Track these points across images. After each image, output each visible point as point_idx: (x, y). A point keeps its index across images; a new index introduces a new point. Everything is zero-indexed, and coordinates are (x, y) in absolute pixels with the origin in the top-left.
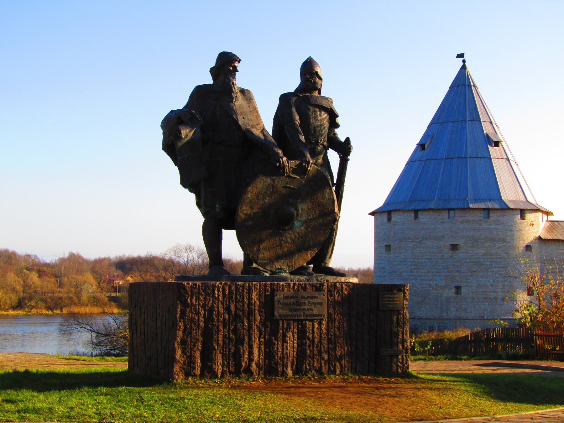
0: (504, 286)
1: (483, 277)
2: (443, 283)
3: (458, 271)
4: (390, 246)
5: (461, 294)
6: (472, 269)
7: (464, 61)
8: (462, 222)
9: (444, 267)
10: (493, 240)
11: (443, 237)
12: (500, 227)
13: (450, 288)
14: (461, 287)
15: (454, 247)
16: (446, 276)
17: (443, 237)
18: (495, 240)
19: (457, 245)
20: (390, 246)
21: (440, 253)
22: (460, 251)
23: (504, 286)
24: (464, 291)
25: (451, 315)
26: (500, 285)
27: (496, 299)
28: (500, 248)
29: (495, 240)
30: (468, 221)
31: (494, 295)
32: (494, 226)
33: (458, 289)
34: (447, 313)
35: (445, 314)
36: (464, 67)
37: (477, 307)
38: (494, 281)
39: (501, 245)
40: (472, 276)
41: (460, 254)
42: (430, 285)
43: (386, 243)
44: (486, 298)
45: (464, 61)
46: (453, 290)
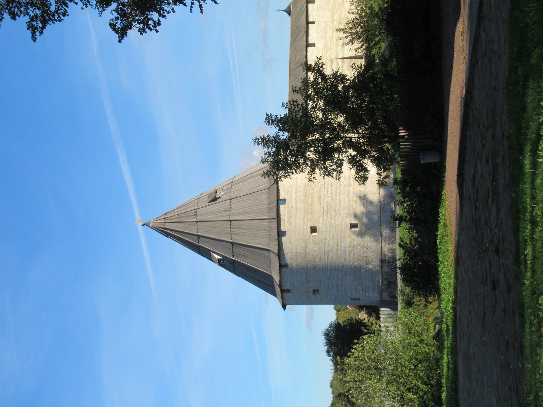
0: (348, 185)
1: (340, 203)
4: (314, 291)
6: (334, 214)
8: (290, 224)
10: (306, 195)
15: (314, 230)
18: (306, 194)
19: (311, 227)
20: (314, 291)
23: (348, 185)
28: (313, 189)
29: (306, 194)
38: (344, 194)
40: (340, 214)
43: (312, 294)
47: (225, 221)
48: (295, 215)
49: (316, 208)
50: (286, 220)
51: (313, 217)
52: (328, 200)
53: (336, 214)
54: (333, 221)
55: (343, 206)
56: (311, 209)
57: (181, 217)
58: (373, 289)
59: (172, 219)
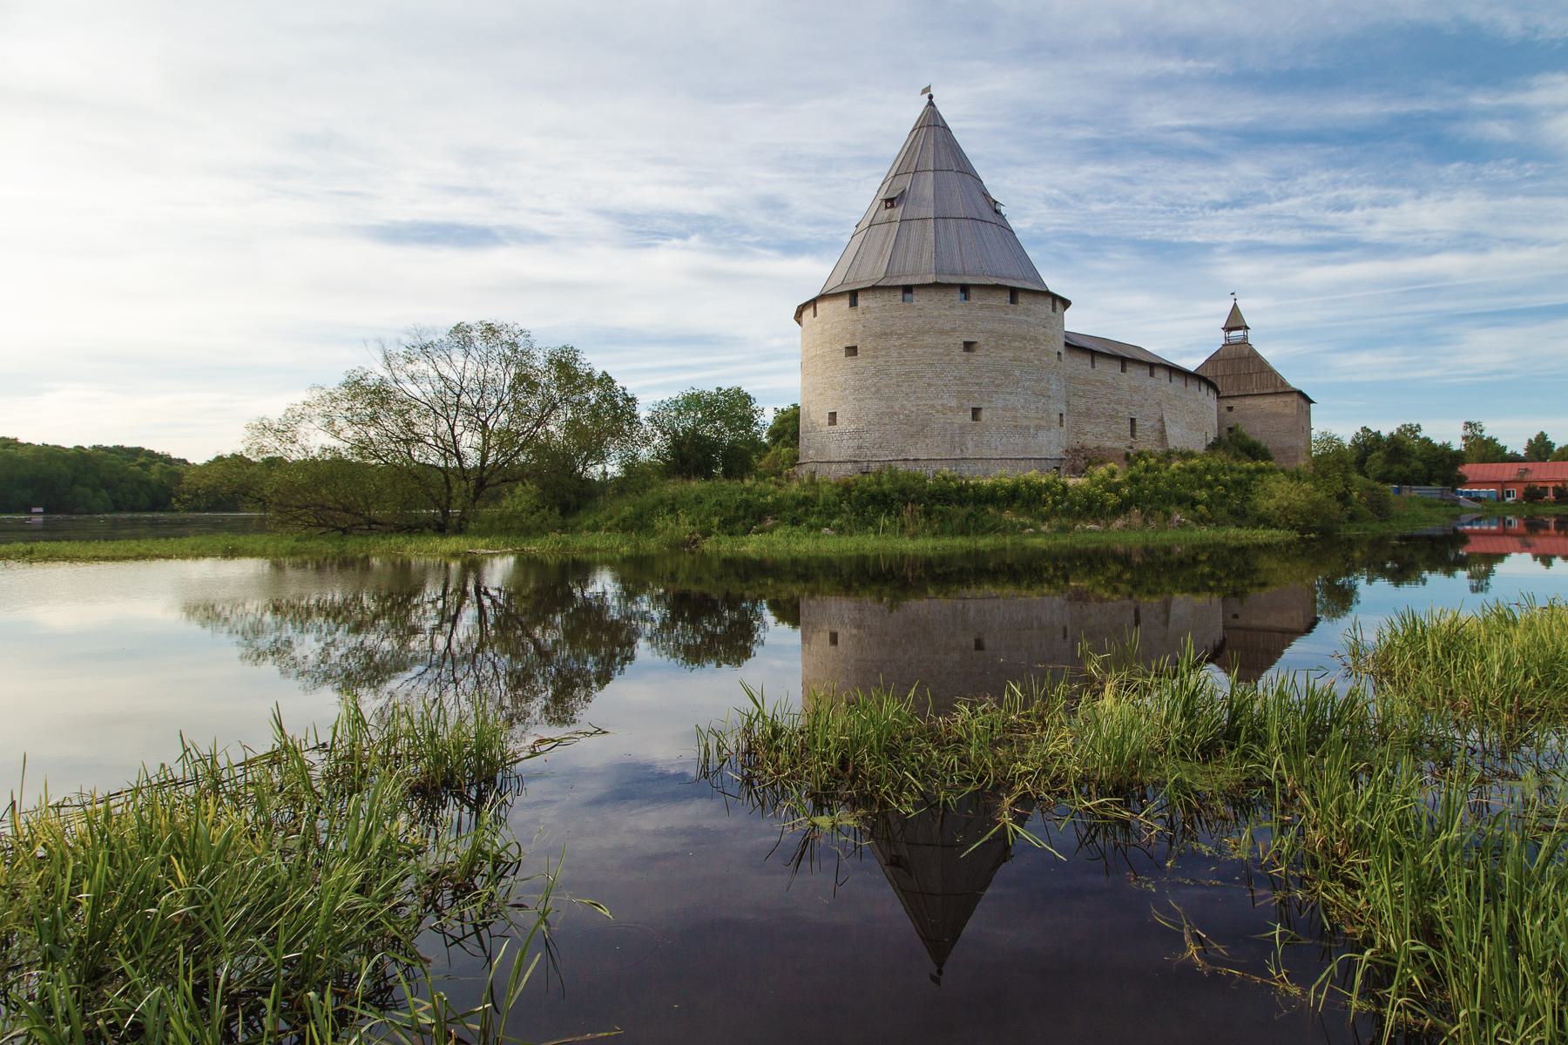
2: (954, 403)
7: (931, 97)
8: (981, 307)
11: (954, 330)
12: (1031, 319)
15: (968, 346)
17: (954, 330)
22: (978, 352)
24: (984, 415)
27: (1028, 428)
30: (990, 307)
31: (1025, 423)
32: (1023, 317)
33: (976, 412)
36: (931, 104)
41: (978, 357)
42: (933, 406)
45: (931, 97)
58: (859, 447)
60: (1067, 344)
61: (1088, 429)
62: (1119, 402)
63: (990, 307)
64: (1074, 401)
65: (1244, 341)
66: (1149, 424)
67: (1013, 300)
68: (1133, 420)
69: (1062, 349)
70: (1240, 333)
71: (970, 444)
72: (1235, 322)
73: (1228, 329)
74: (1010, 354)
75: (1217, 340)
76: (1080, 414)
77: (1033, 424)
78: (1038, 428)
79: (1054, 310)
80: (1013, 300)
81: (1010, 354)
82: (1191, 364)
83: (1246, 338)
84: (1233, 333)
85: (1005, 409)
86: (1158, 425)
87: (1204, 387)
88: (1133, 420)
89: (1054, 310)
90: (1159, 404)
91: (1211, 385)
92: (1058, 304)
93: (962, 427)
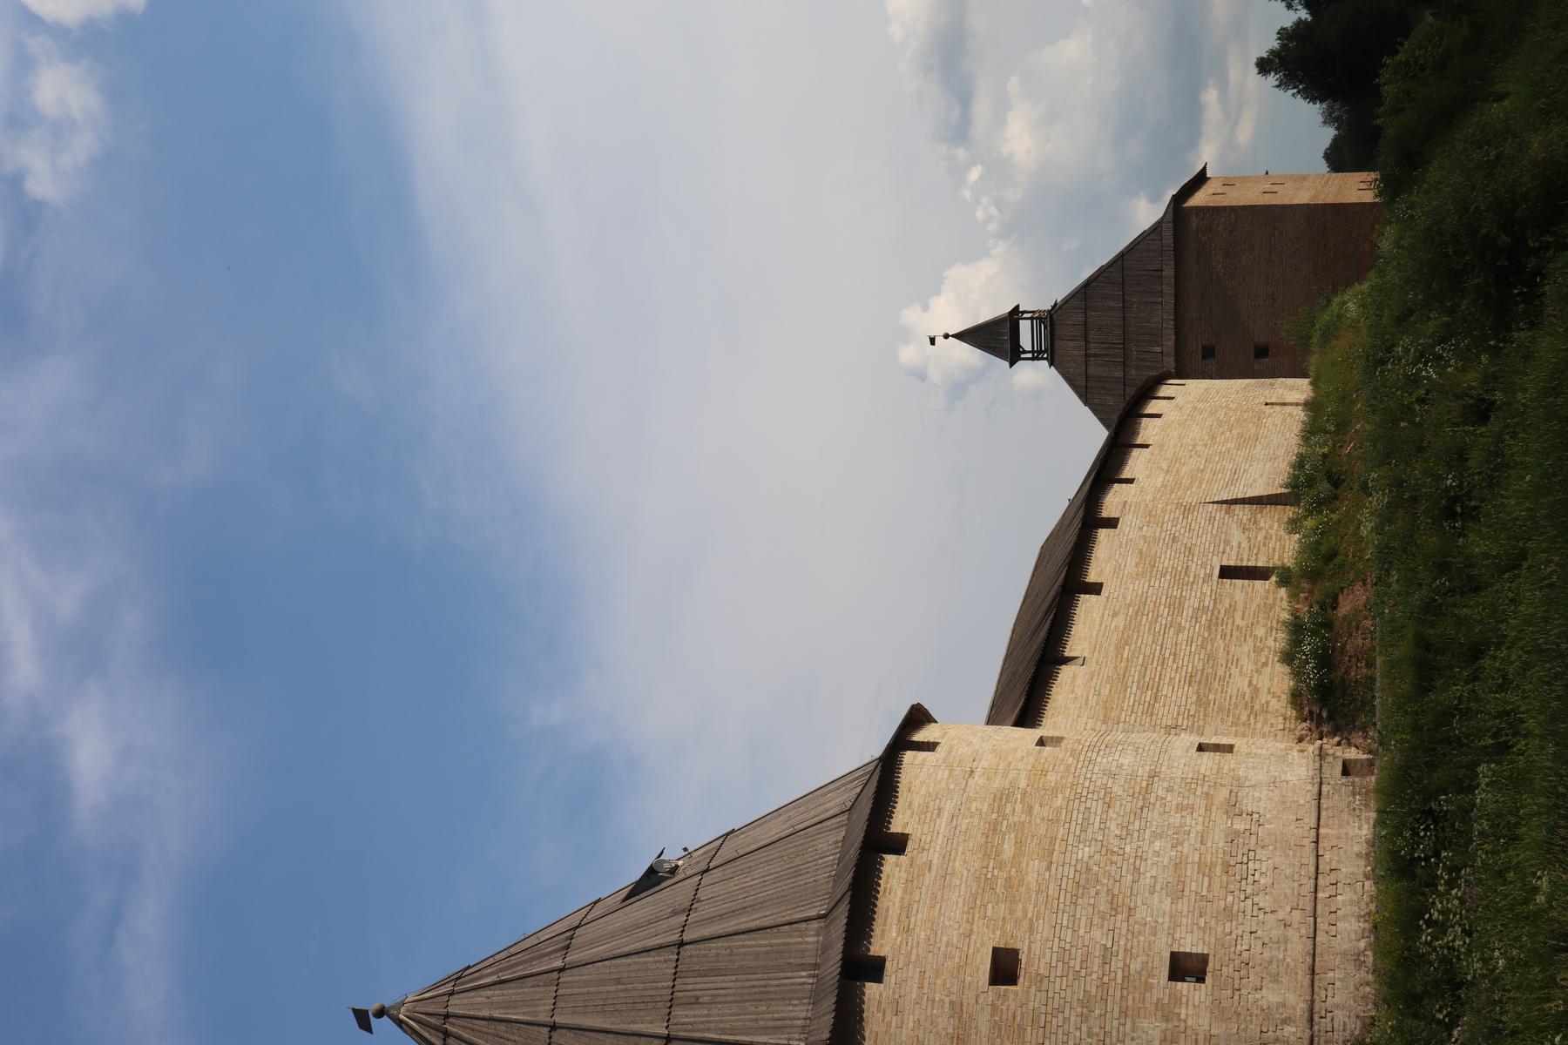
3: (1105, 962)
5: (1204, 959)
6: (1103, 906)
8: (907, 930)
9: (1084, 1018)
10: (994, 828)
12: (948, 807)
13: (1176, 999)
14: (1175, 957)
15: (1005, 968)
16: (1124, 1013)
19: (997, 953)
21: (1022, 1029)
22: (1021, 945)
24: (1190, 944)
25: (1297, 1003)
26: (1176, 819)
27: (1233, 838)
30: (907, 910)
31: (1218, 840)
33: (1186, 968)
34: (1285, 1021)
35: (1289, 1030)
37: (1264, 901)
39: (1018, 807)
40: (1131, 911)
41: (1035, 957)
44: (1227, 868)
46: (1182, 986)
47: (661, 947)
48: (934, 896)
49: (1031, 878)
50: (894, 913)
51: (1011, 912)
52: (1084, 852)
53: (1114, 909)
54: (1097, 934)
55: (1146, 880)
56: (1009, 878)
57: (513, 966)
59: (481, 978)
60: (1019, 723)
61: (1240, 683)
62: (1177, 606)
63: (907, 910)
64: (1165, 714)
65: (1050, 321)
66: (1237, 536)
67: (898, 845)
68: (1227, 573)
69: (1029, 735)
70: (1025, 327)
71: (1270, 996)
72: (996, 337)
73: (1014, 355)
74: (1033, 869)
75: (1036, 376)
76: (1201, 702)
77: (1221, 822)
78: (1233, 808)
79: (930, 747)
80: (898, 845)
81: (1033, 869)
82: (1089, 435)
83: (1038, 318)
84: (1026, 341)
85: (1177, 893)
86: (1242, 512)
87: (1153, 407)
88: (1227, 573)
89: (930, 747)
90: (1187, 510)
91: (1148, 391)
92: (919, 737)
93: (1219, 1011)
